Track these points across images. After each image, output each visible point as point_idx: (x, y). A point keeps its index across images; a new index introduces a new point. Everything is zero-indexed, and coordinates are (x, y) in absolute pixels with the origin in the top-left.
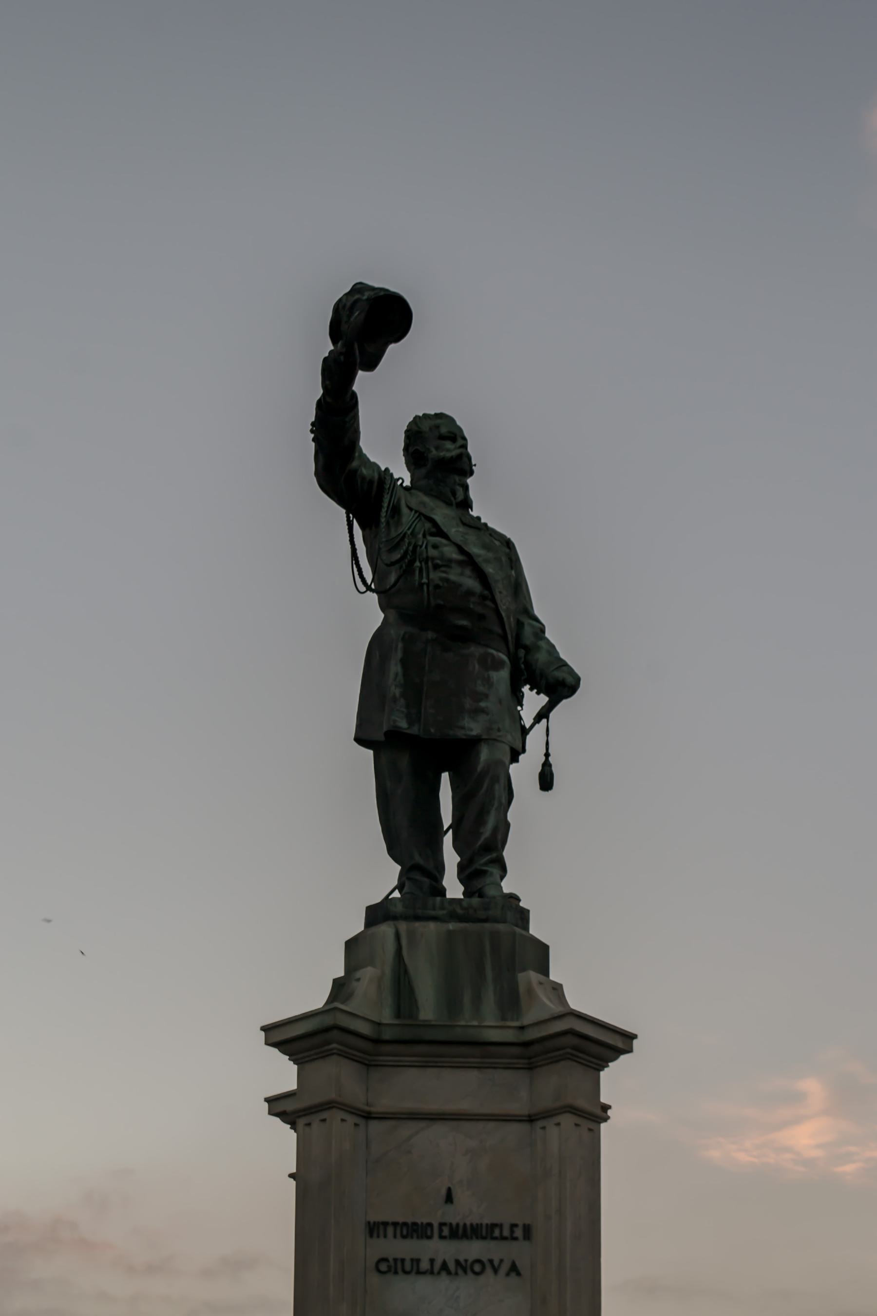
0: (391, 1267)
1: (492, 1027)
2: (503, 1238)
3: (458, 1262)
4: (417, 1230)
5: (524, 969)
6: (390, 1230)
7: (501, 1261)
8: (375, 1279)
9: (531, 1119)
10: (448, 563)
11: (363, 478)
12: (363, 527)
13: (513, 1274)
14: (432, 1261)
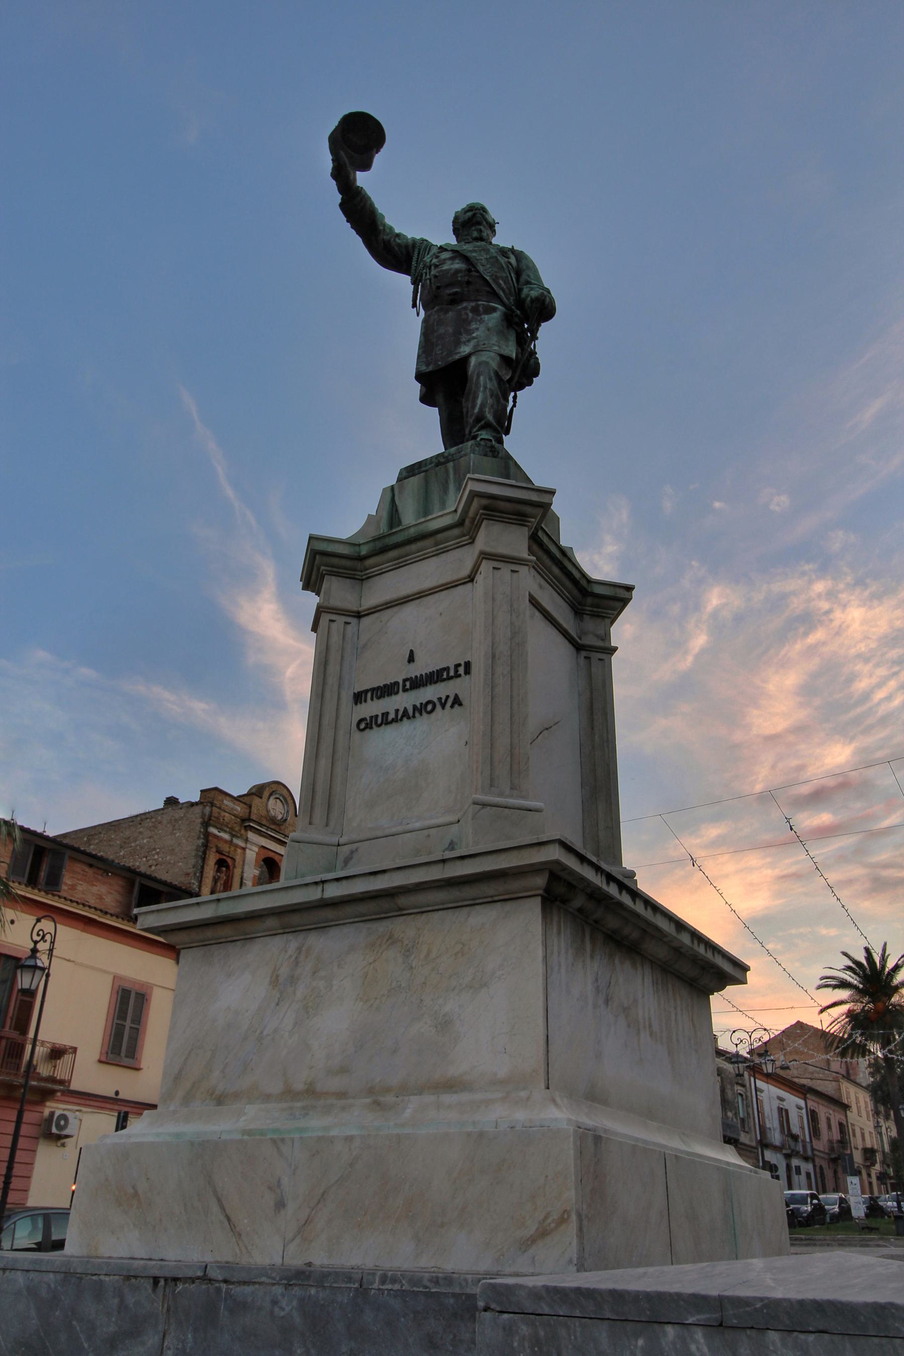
2: (450, 678)
3: (415, 707)
4: (388, 690)
7: (448, 697)
8: (357, 735)
11: (399, 245)
13: (456, 706)
14: (397, 711)
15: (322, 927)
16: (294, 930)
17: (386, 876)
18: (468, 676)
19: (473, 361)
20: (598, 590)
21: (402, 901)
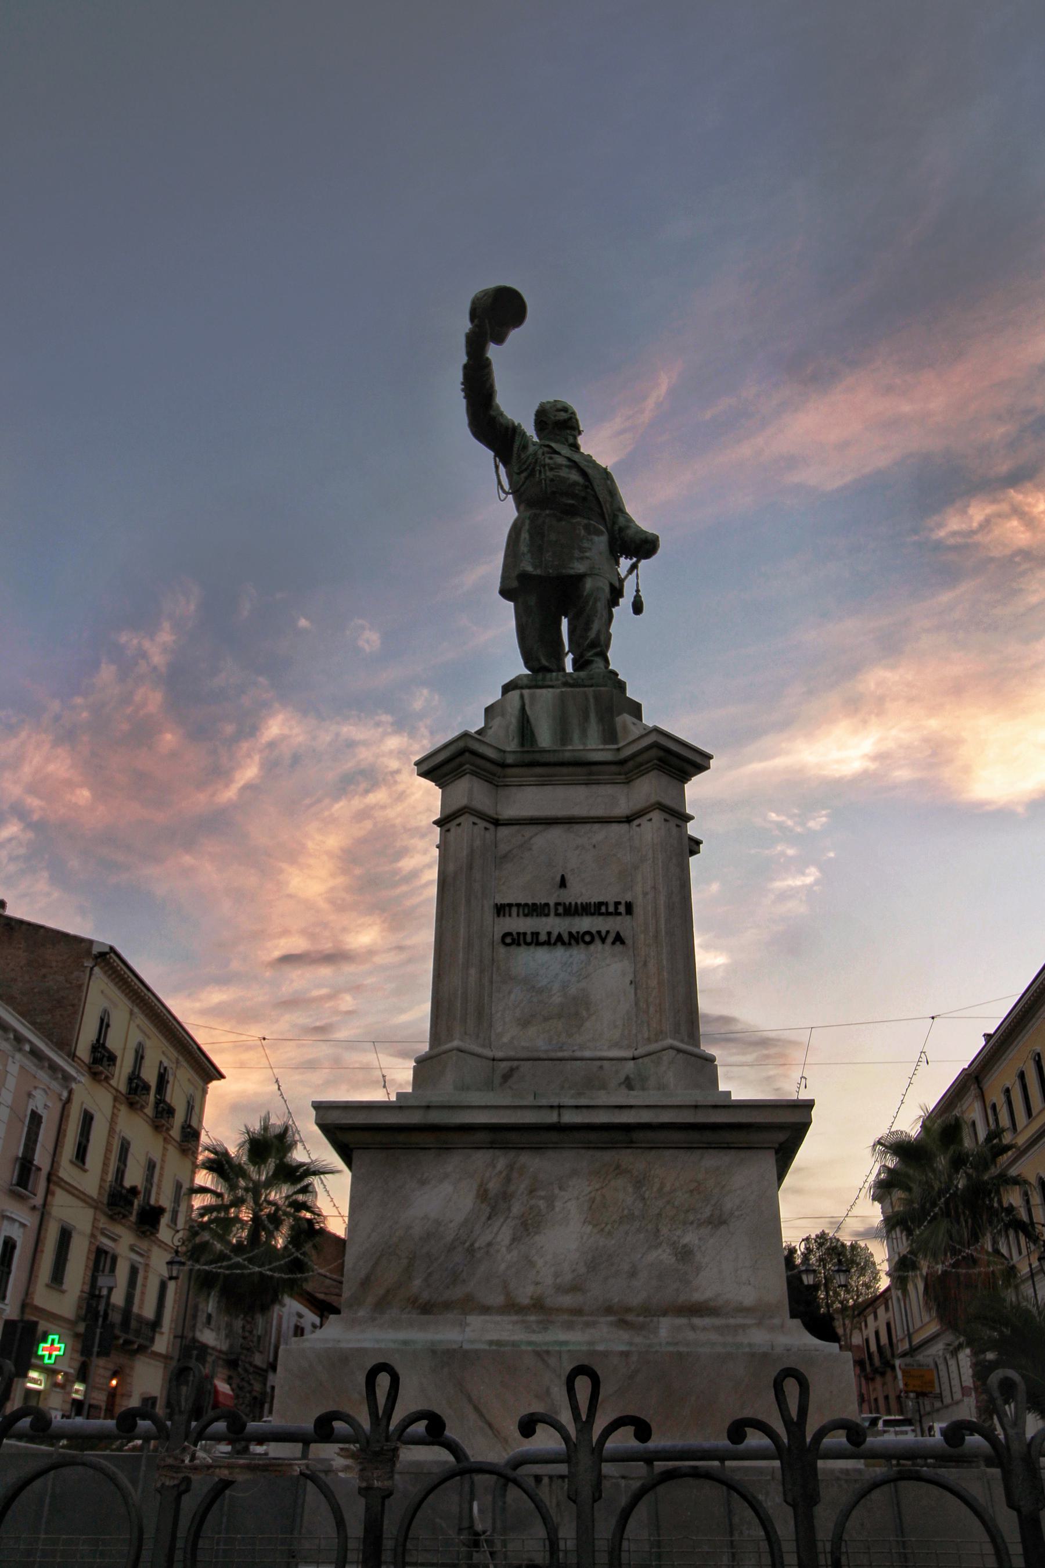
1: (591, 745)
2: (608, 914)
5: (619, 714)
6: (514, 910)
7: (608, 932)
8: (502, 950)
9: (628, 820)
10: (560, 467)
12: (505, 465)
13: (618, 943)
14: (549, 934)
15: (537, 1148)
16: (506, 1147)
17: (633, 1112)
18: (628, 917)
19: (589, 584)
21: (638, 1136)
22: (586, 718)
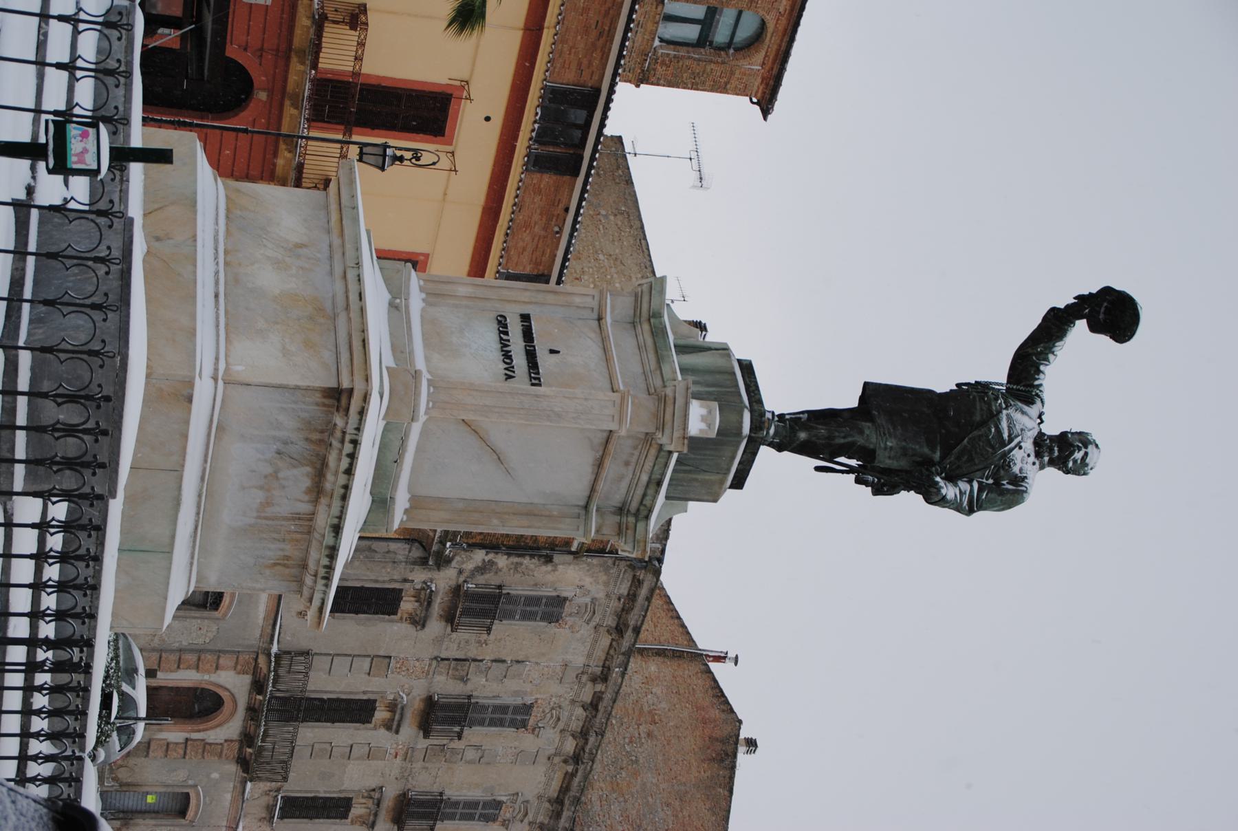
0: (502, 324)
4: (528, 335)
8: (494, 315)
20: (640, 526)
22: (708, 386)
